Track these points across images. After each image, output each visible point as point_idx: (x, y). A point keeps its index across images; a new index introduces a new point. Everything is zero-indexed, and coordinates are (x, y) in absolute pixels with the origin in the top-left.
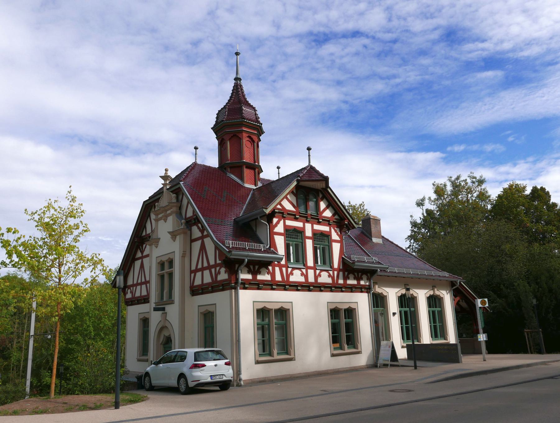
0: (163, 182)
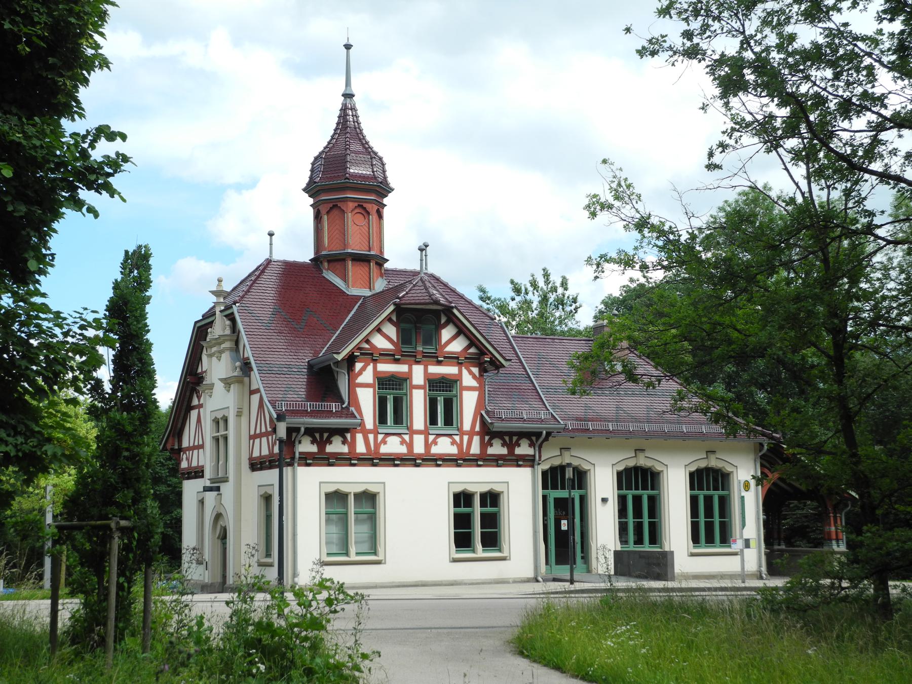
0: (214, 299)
